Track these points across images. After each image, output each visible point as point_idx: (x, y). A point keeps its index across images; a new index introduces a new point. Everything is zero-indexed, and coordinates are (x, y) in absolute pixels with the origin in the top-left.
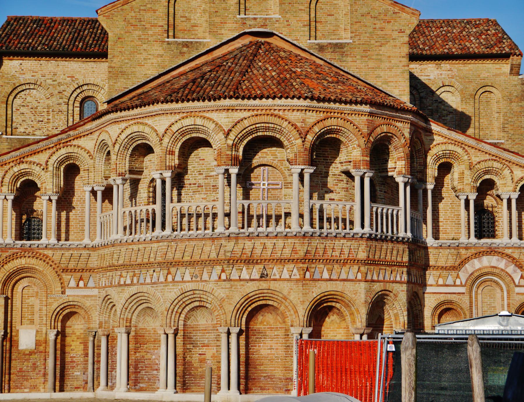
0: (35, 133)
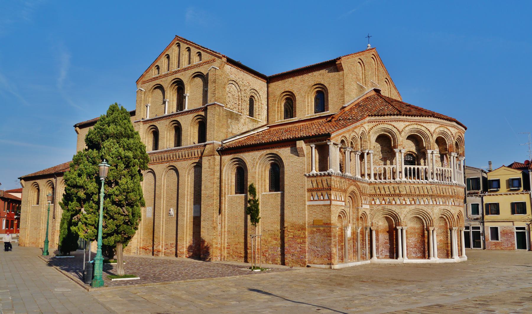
0: (234, 109)
